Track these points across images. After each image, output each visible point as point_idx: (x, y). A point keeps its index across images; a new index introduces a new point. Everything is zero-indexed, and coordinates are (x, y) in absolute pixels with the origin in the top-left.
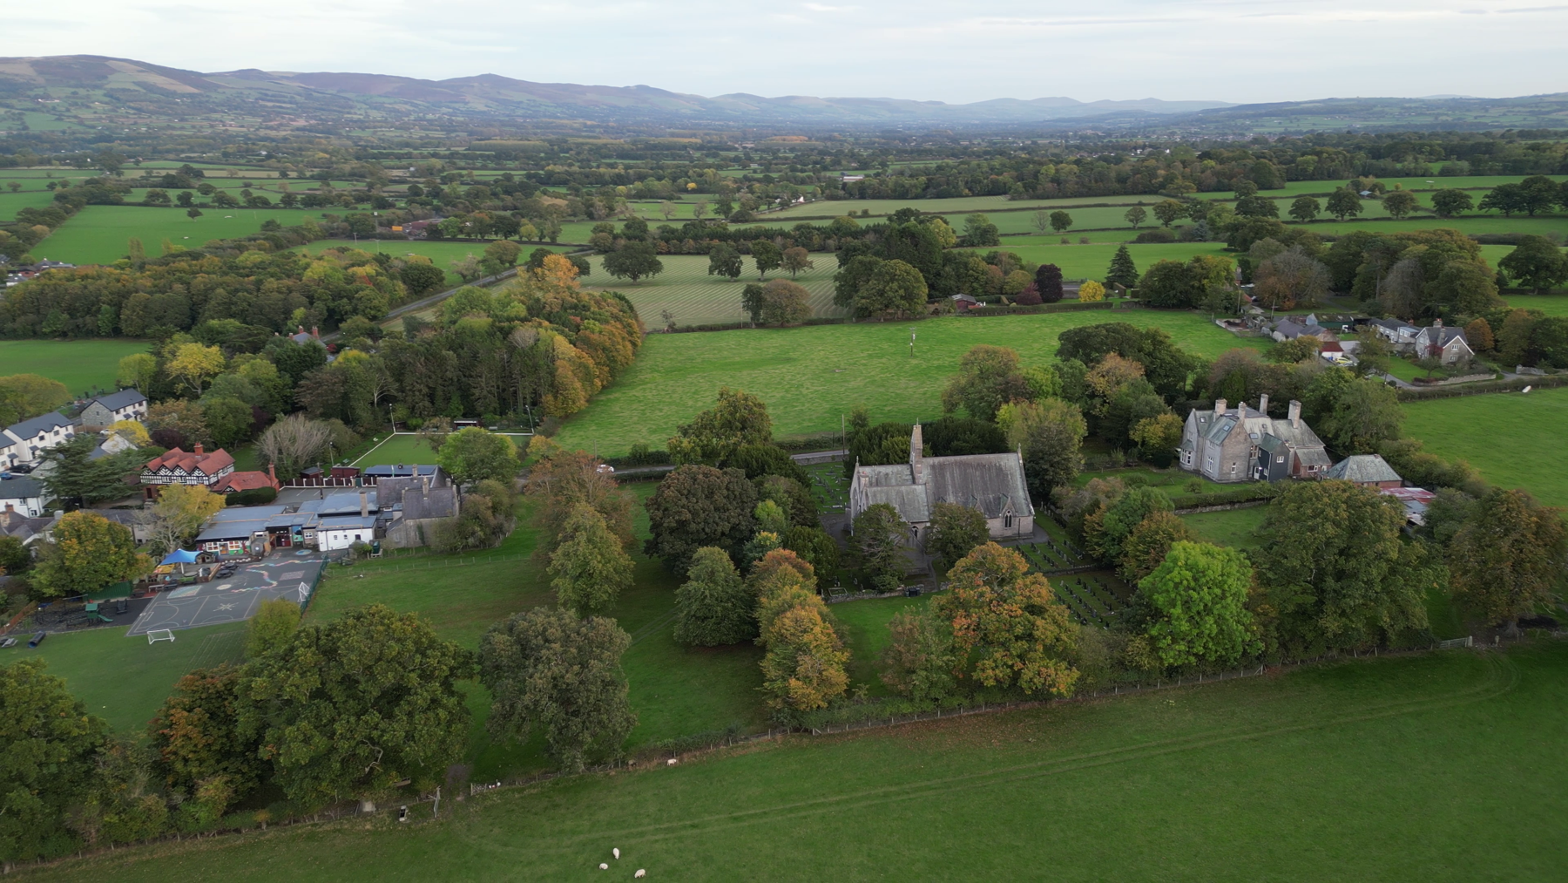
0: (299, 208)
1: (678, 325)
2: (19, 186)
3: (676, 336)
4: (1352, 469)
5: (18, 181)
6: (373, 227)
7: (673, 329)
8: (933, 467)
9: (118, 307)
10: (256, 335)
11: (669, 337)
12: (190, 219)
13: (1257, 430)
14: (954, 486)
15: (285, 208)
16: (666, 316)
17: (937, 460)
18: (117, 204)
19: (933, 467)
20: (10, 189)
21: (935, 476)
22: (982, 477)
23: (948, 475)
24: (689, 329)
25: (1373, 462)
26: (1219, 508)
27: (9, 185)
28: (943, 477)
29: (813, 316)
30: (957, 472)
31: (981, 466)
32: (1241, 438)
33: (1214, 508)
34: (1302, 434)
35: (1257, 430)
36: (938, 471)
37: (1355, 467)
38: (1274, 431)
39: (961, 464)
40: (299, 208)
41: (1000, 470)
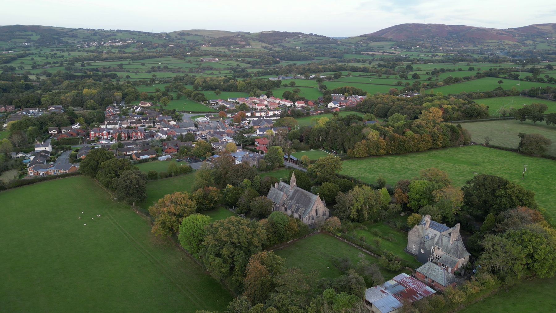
0: (553, 83)
1: (491, 143)
2: (480, 69)
3: (489, 149)
4: (425, 267)
5: (480, 67)
6: (538, 93)
7: (487, 145)
8: (295, 190)
9: (375, 106)
10: (351, 118)
11: (485, 148)
12: (499, 84)
13: (430, 236)
14: (296, 199)
15: (548, 83)
16: (487, 139)
17: (298, 188)
18: (497, 77)
19: (295, 190)
20: (477, 70)
21: (294, 193)
22: (304, 199)
23: (297, 194)
24: (493, 147)
25: (438, 270)
26: (369, 252)
27: (478, 69)
28: (296, 194)
29: (547, 153)
30: (299, 194)
31: (306, 195)
32: (417, 234)
33: (367, 252)
34: (452, 248)
35: (430, 236)
36: (296, 191)
37: (427, 267)
38: (438, 240)
39: (302, 193)
40: (553, 83)
41: (310, 199)
